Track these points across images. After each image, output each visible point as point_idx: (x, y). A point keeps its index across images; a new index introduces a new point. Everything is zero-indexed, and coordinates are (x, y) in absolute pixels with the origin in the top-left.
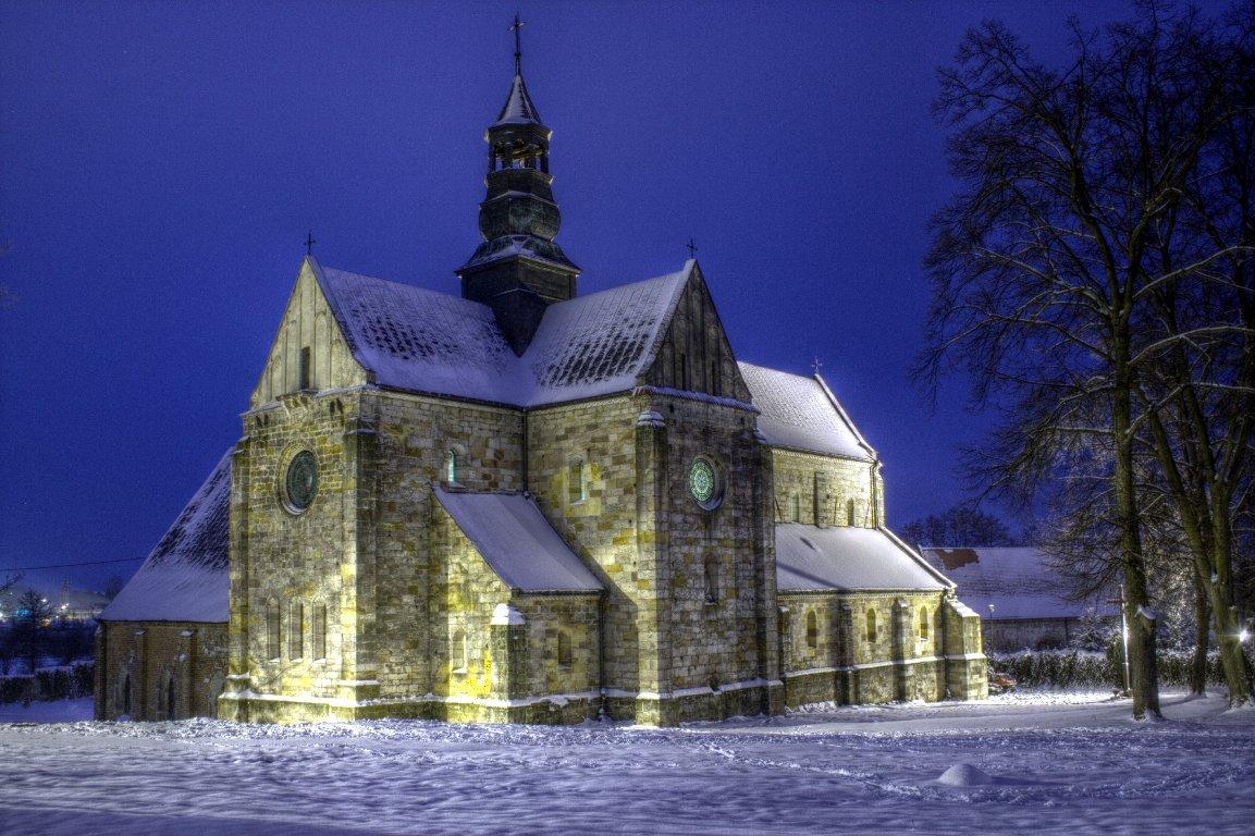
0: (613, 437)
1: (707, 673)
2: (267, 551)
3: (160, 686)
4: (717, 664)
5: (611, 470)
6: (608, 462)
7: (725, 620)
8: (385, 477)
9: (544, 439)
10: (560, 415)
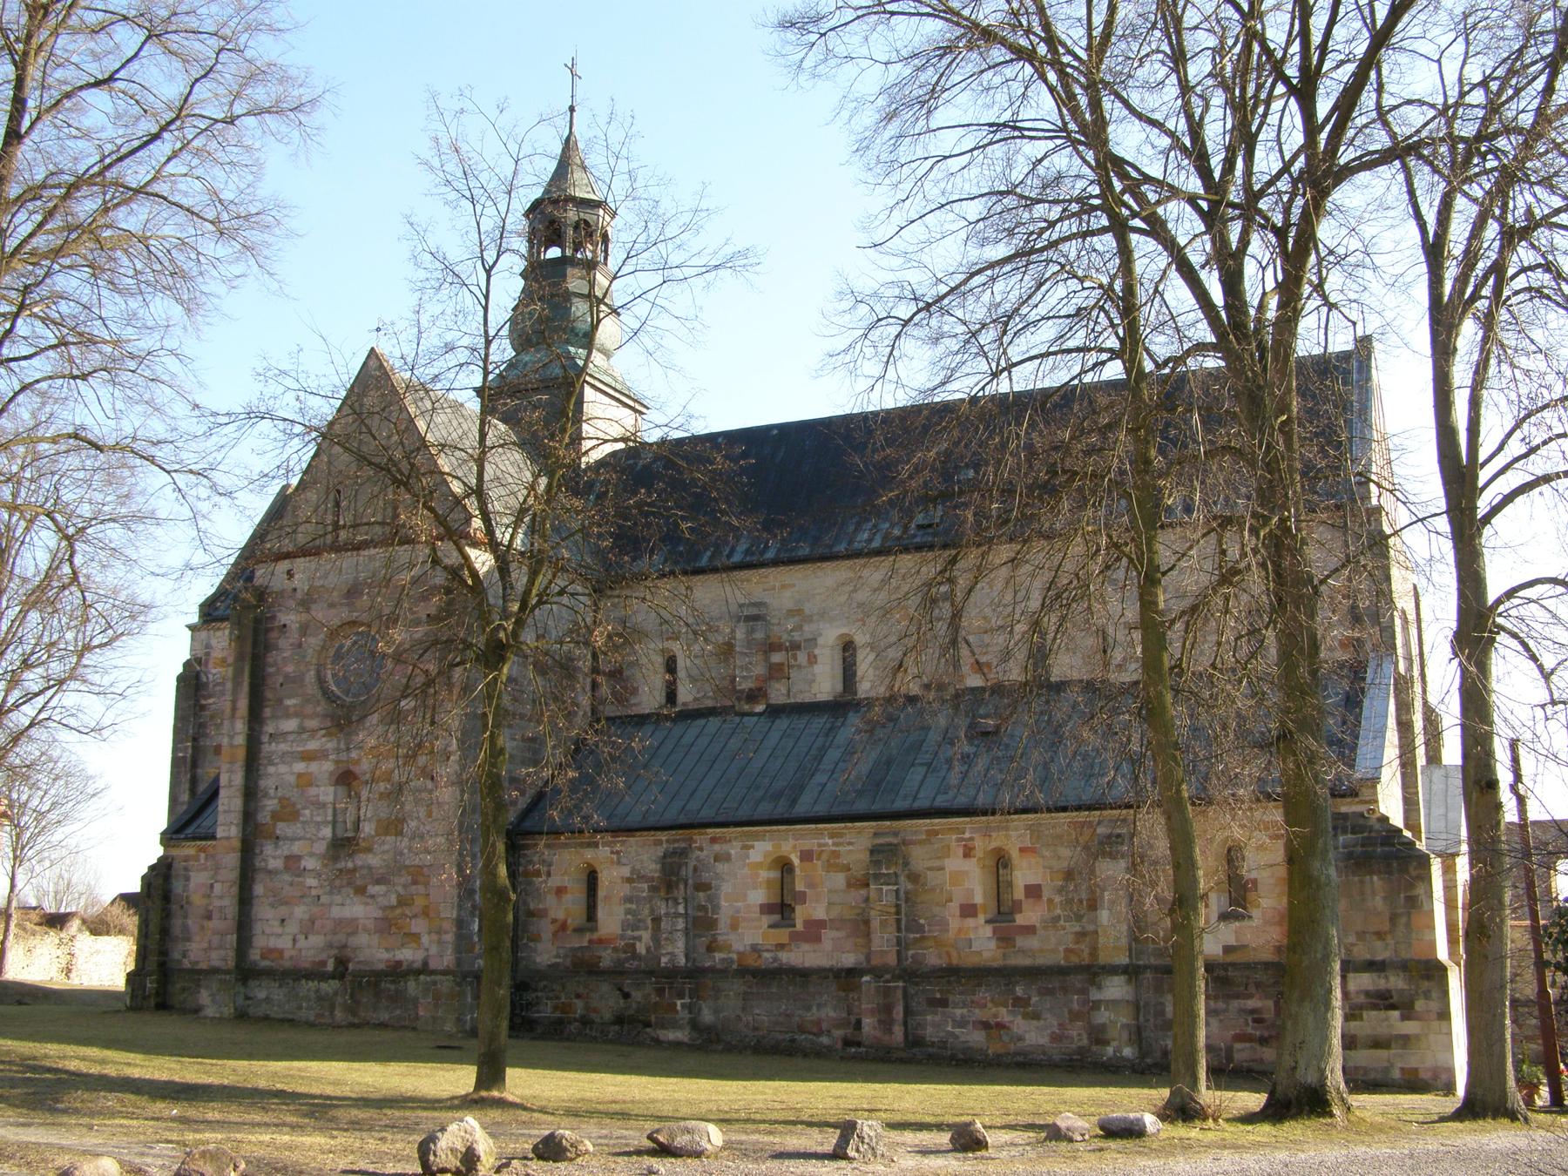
1: (330, 946)
4: (348, 935)
7: (370, 868)
8: (212, 717)
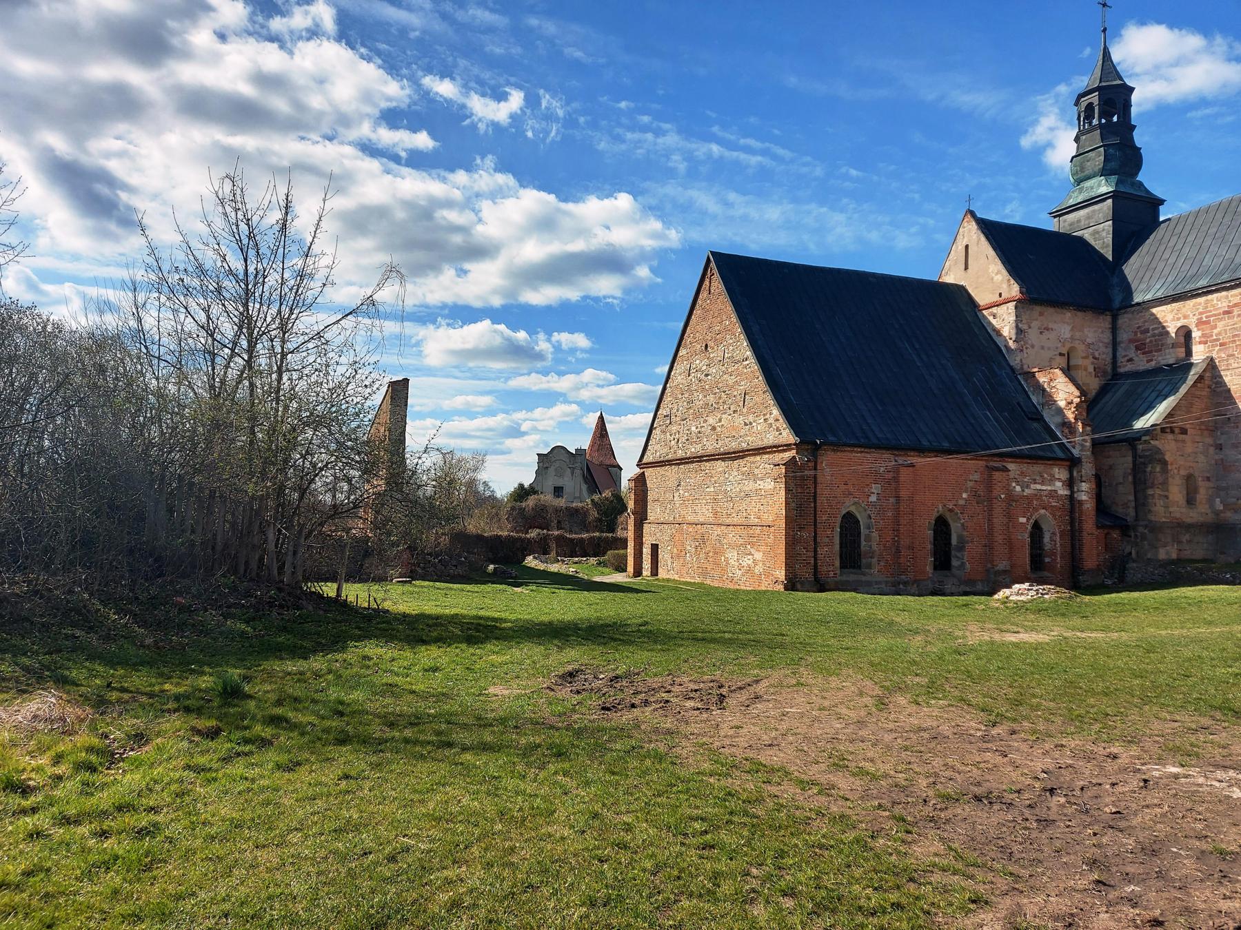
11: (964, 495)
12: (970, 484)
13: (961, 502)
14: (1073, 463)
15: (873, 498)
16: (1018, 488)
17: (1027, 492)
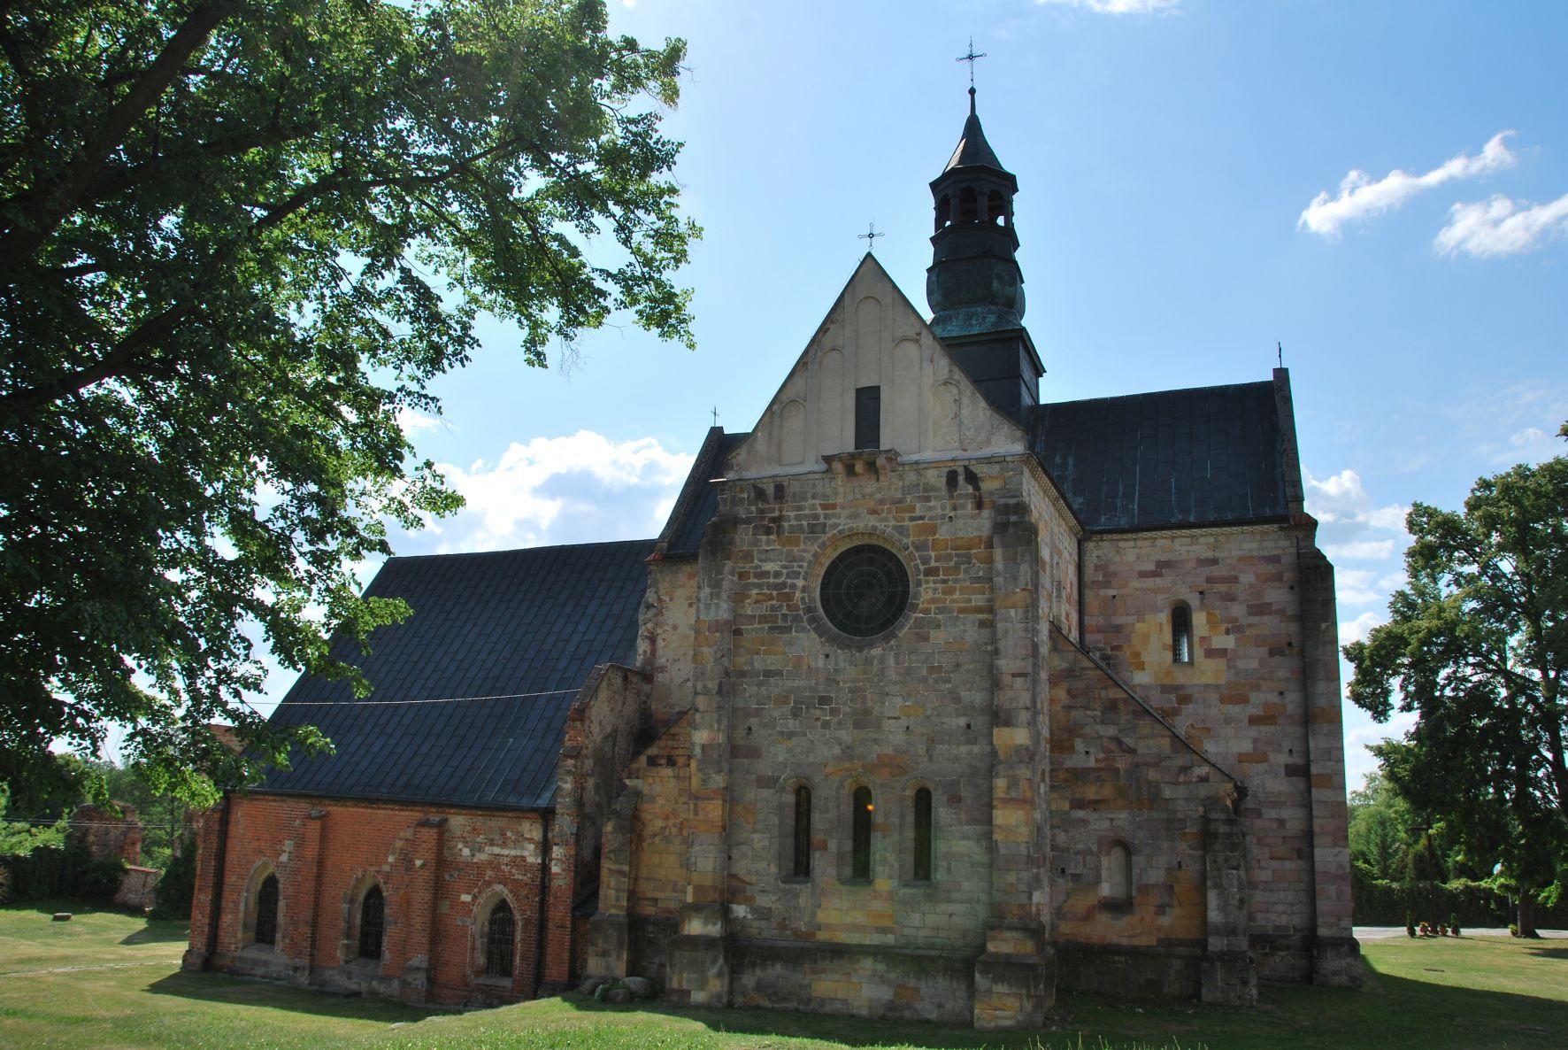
0: (1247, 578)
2: (782, 700)
3: (352, 901)
5: (1244, 621)
6: (1238, 610)
9: (1115, 574)
10: (1146, 543)
11: (391, 859)
12: (399, 844)
13: (386, 868)
14: (547, 816)
15: (284, 858)
16: (466, 852)
17: (481, 857)
